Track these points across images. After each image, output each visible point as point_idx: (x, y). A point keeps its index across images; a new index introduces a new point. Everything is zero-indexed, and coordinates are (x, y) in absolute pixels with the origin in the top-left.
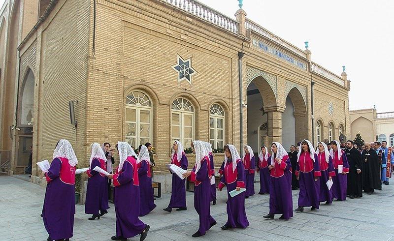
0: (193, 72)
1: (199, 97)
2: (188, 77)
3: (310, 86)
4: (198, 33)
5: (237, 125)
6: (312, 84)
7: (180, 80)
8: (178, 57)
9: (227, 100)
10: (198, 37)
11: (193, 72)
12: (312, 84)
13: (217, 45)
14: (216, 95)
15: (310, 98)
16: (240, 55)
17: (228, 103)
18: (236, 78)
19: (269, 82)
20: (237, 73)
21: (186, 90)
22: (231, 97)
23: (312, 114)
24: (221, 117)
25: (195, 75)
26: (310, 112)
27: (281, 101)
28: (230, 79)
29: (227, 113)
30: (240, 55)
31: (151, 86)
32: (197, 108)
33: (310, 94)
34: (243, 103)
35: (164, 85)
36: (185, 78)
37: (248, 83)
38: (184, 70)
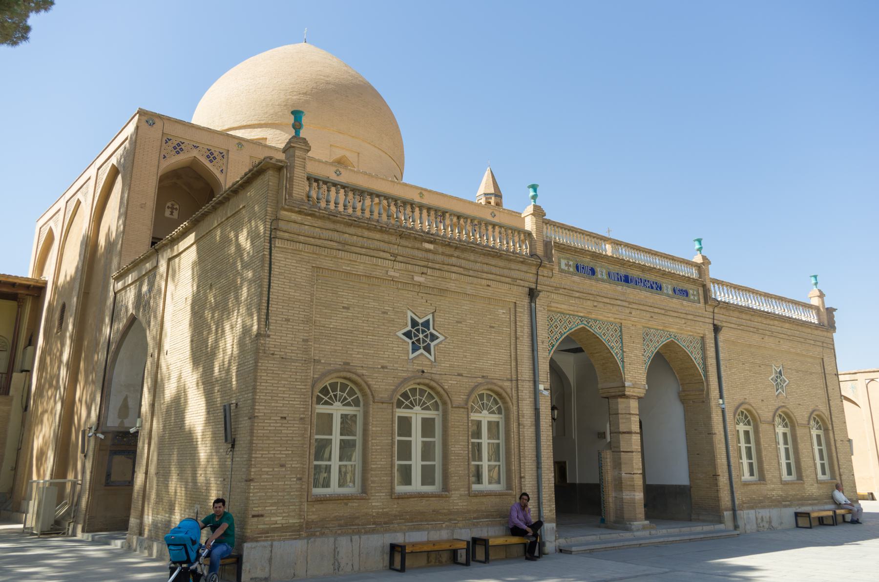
0: (437, 338)
1: (450, 383)
2: (427, 349)
3: (710, 335)
4: (446, 267)
5: (528, 432)
6: (717, 329)
7: (411, 356)
8: (410, 314)
9: (507, 384)
10: (447, 274)
11: (437, 338)
12: (717, 329)
13: (484, 282)
14: (483, 377)
15: (711, 362)
16: (532, 294)
17: (509, 390)
18: (525, 340)
19: (604, 339)
20: (527, 330)
21: (423, 372)
22: (514, 377)
23: (721, 397)
24: (495, 418)
25: (441, 343)
26: (714, 393)
27: (635, 375)
28: (513, 341)
29: (507, 409)
30: (532, 294)
31: (360, 371)
32: (444, 403)
33: (711, 353)
34: (541, 387)
35: (383, 367)
36: (422, 351)
37: (553, 346)
38: (421, 336)
